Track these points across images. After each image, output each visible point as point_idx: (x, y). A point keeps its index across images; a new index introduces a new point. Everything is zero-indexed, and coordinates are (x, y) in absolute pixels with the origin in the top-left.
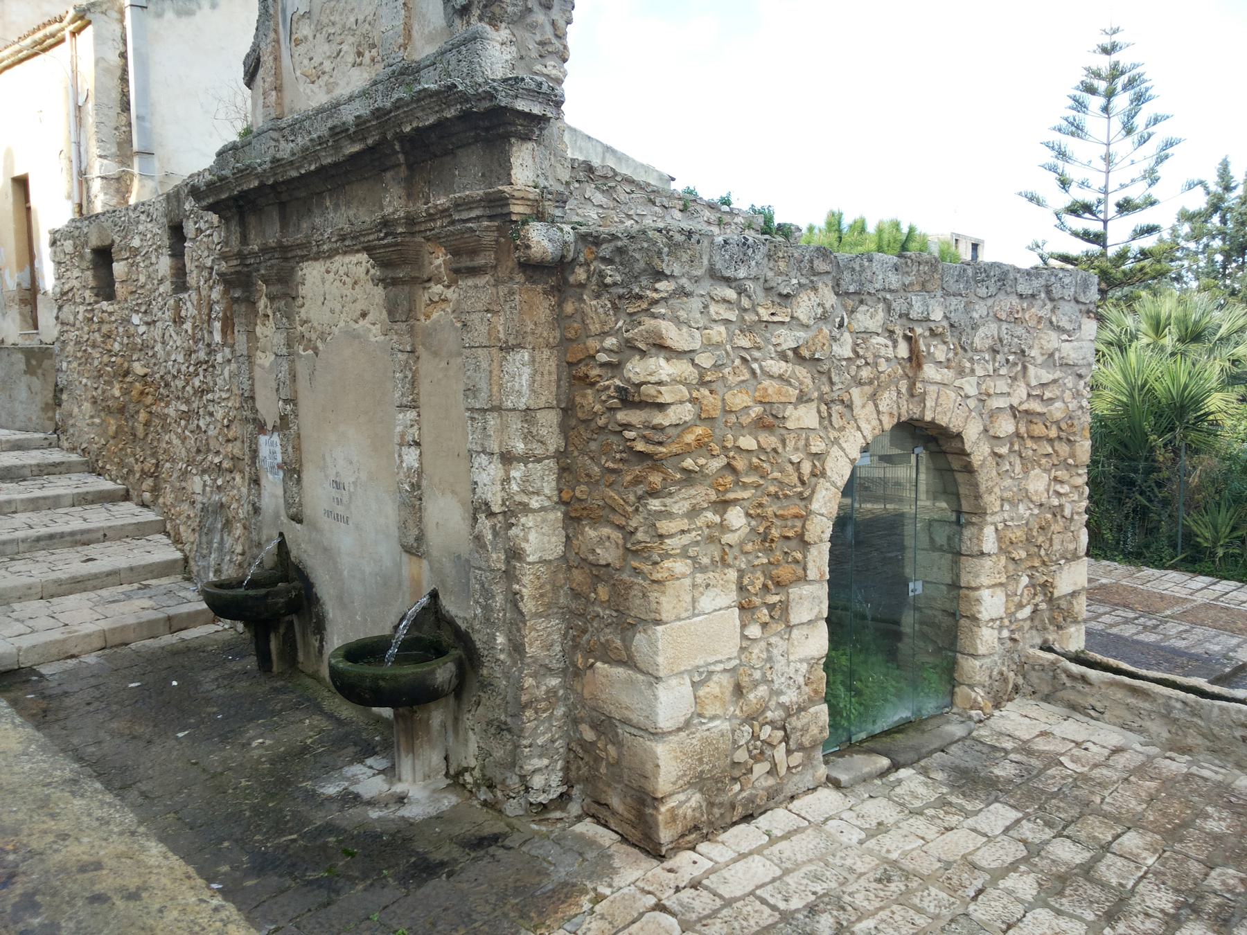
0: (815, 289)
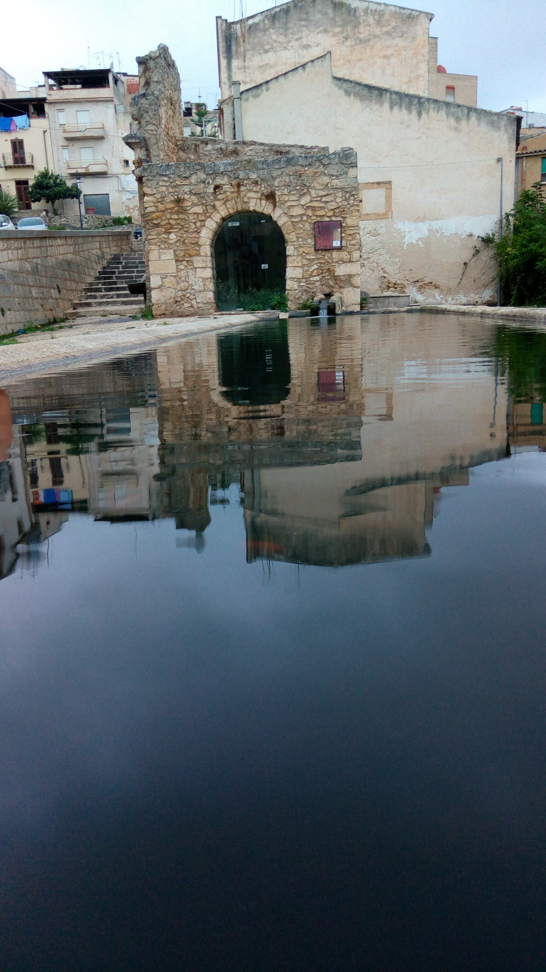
0: (197, 174)
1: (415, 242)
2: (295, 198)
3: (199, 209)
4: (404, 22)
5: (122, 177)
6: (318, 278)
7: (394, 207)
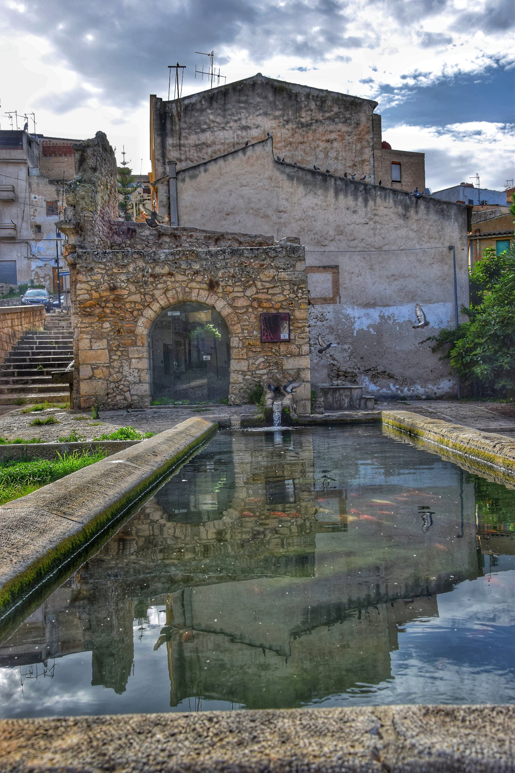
1: (365, 329)
2: (241, 290)
3: (137, 298)
4: (346, 109)
5: (33, 243)
6: (265, 371)
7: (342, 292)
